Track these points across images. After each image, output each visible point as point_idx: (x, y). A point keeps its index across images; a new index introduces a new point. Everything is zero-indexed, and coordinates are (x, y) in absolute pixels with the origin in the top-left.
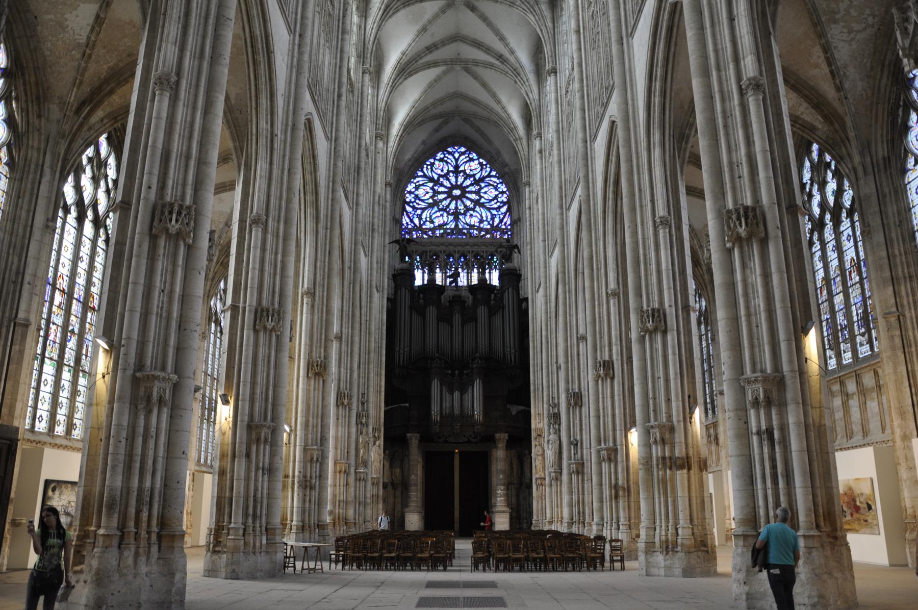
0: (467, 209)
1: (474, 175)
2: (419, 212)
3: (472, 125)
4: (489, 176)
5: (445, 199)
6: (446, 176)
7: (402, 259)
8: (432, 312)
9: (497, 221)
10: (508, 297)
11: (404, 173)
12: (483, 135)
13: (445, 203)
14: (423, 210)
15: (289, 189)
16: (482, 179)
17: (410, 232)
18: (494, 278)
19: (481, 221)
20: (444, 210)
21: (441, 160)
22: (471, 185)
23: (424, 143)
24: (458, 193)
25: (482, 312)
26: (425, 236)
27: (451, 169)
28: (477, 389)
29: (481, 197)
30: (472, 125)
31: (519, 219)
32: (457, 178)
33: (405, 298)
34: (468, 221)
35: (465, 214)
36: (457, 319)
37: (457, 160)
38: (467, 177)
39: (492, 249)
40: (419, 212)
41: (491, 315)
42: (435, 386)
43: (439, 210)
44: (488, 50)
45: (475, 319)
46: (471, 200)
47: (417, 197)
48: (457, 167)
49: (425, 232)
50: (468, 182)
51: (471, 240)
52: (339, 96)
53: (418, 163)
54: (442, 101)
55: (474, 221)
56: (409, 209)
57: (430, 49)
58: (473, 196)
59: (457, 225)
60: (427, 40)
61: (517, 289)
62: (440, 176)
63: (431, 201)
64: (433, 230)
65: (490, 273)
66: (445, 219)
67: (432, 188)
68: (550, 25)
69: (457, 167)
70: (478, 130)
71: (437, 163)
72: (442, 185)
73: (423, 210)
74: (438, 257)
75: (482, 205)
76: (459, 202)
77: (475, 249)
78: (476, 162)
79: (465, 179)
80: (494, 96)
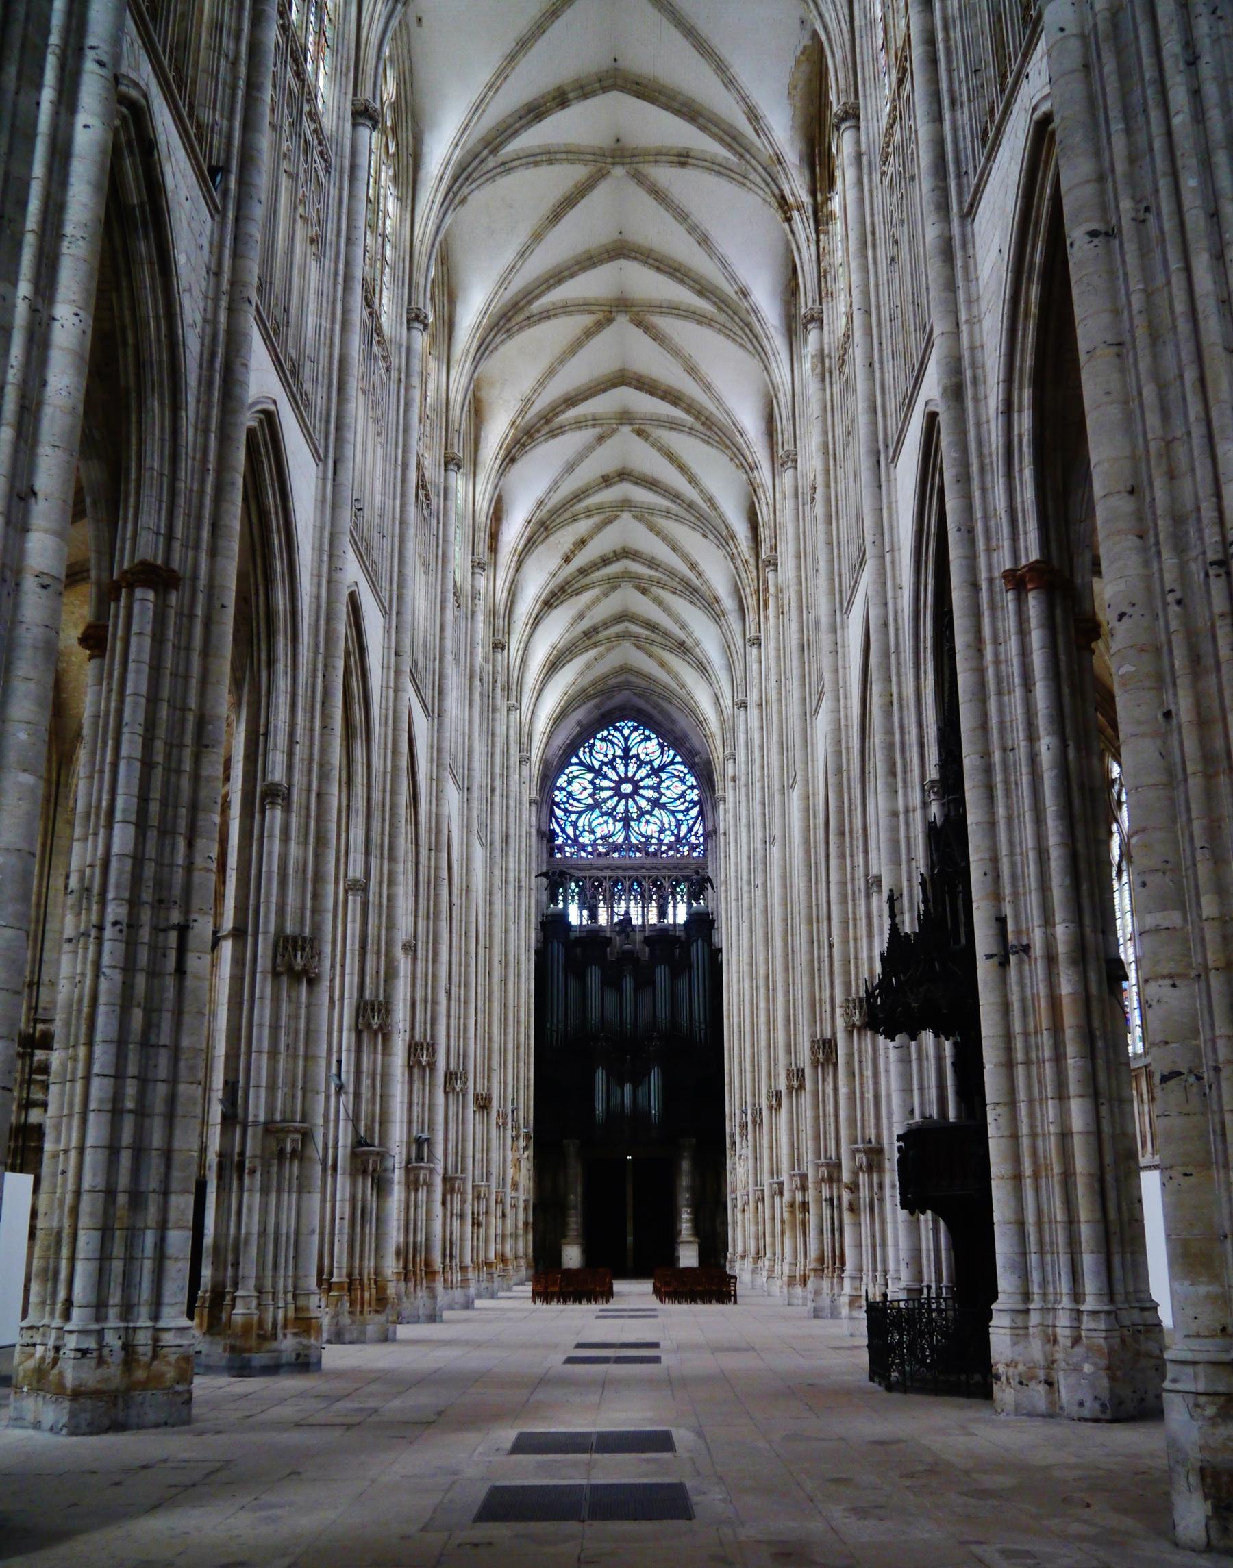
0: (642, 813)
1: (651, 762)
2: (573, 817)
3: (647, 701)
4: (672, 763)
5: (611, 797)
6: (611, 764)
7: (554, 900)
8: (594, 976)
9: (684, 829)
10: (698, 950)
11: (550, 772)
12: (663, 712)
13: (611, 803)
14: (580, 813)
15: (467, 953)
16: (662, 768)
17: (560, 849)
18: (679, 914)
19: (662, 831)
20: (610, 814)
21: (604, 739)
22: (648, 776)
23: (579, 723)
24: (626, 788)
25: (662, 973)
26: (583, 854)
27: (619, 752)
28: (654, 1079)
29: (662, 794)
30: (647, 701)
31: (715, 831)
32: (626, 765)
33: (557, 949)
34: (643, 831)
35: (638, 820)
36: (628, 983)
37: (626, 739)
38: (641, 764)
39: (675, 874)
40: (573, 817)
41: (674, 977)
42: (600, 1076)
43: (603, 814)
44: (666, 634)
45: (651, 983)
46: (648, 800)
47: (570, 795)
48: (626, 750)
49: (583, 847)
50: (643, 773)
51: (649, 861)
52: (493, 790)
53: (572, 749)
54: (605, 677)
55: (652, 830)
56: (559, 813)
57: (587, 634)
58: (650, 794)
59: (627, 838)
60: (585, 624)
61: (708, 940)
62: (603, 763)
63: (590, 801)
64: (594, 844)
65: (675, 907)
66: (611, 827)
67: (592, 782)
68: (740, 642)
69: (626, 750)
70: (656, 706)
71: (598, 743)
72: (605, 777)
73: (580, 813)
74: (600, 885)
75: (663, 807)
76: (630, 802)
77: (654, 874)
78: (655, 741)
79: (639, 768)
80: (676, 677)
